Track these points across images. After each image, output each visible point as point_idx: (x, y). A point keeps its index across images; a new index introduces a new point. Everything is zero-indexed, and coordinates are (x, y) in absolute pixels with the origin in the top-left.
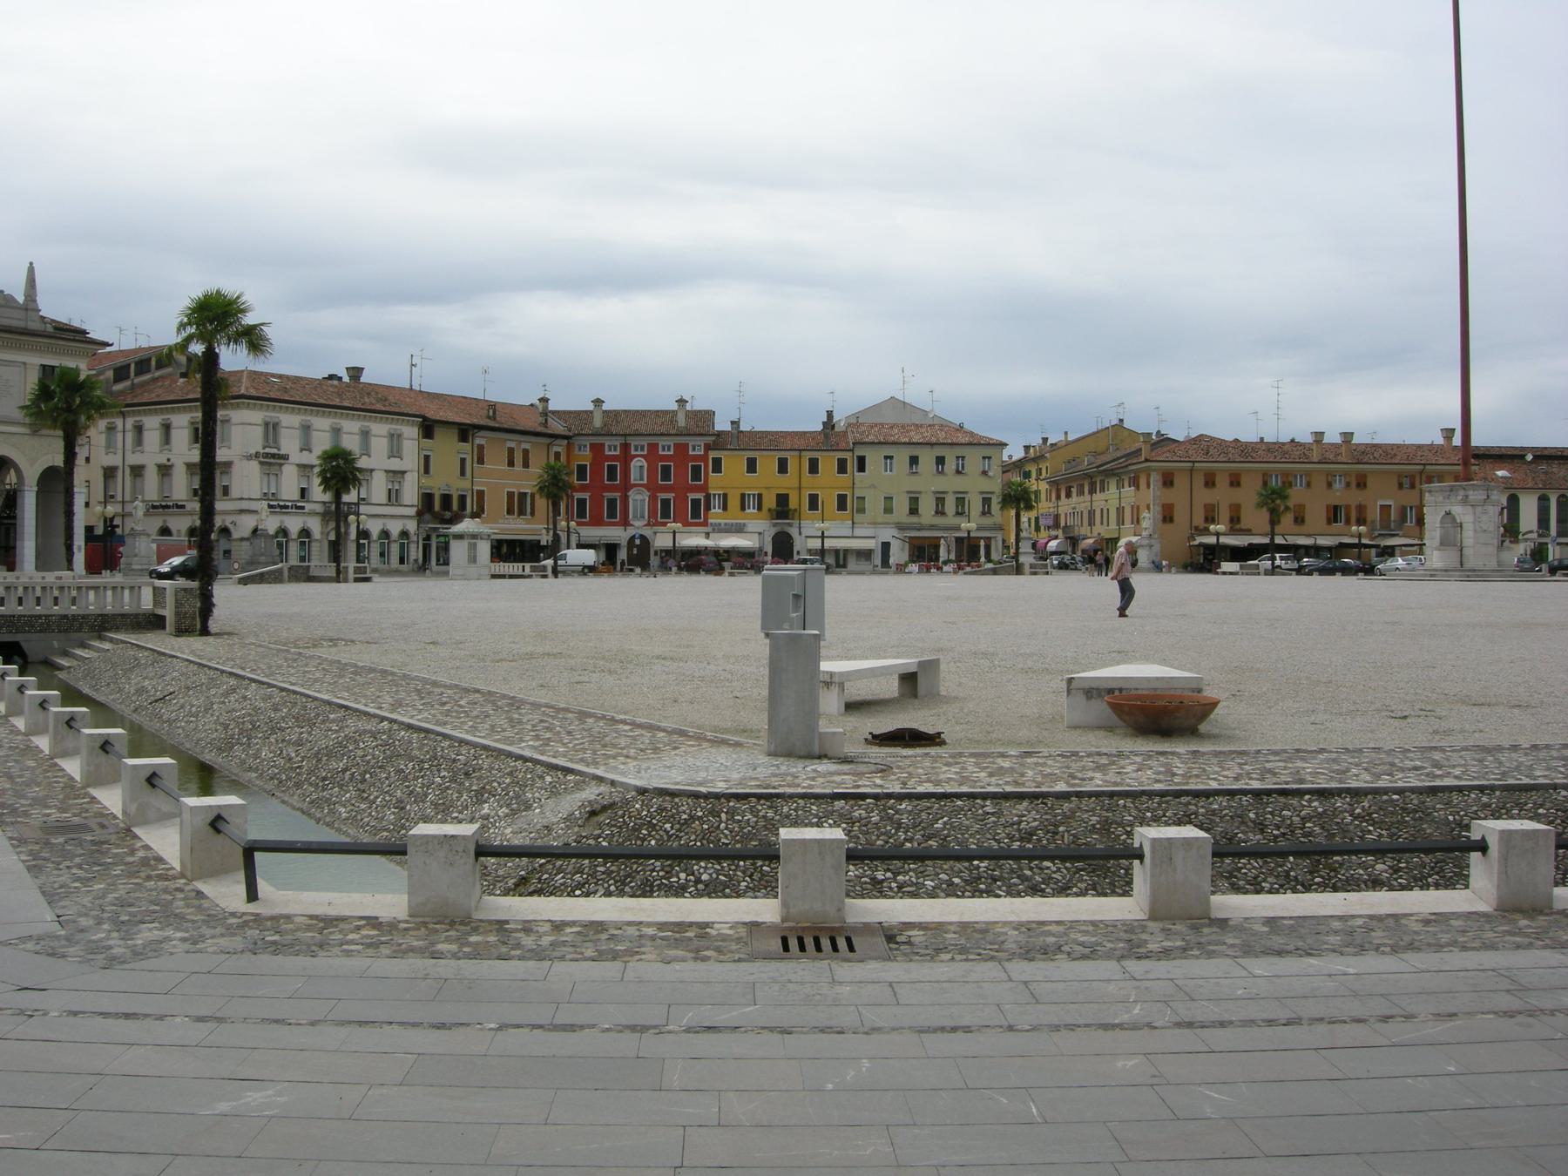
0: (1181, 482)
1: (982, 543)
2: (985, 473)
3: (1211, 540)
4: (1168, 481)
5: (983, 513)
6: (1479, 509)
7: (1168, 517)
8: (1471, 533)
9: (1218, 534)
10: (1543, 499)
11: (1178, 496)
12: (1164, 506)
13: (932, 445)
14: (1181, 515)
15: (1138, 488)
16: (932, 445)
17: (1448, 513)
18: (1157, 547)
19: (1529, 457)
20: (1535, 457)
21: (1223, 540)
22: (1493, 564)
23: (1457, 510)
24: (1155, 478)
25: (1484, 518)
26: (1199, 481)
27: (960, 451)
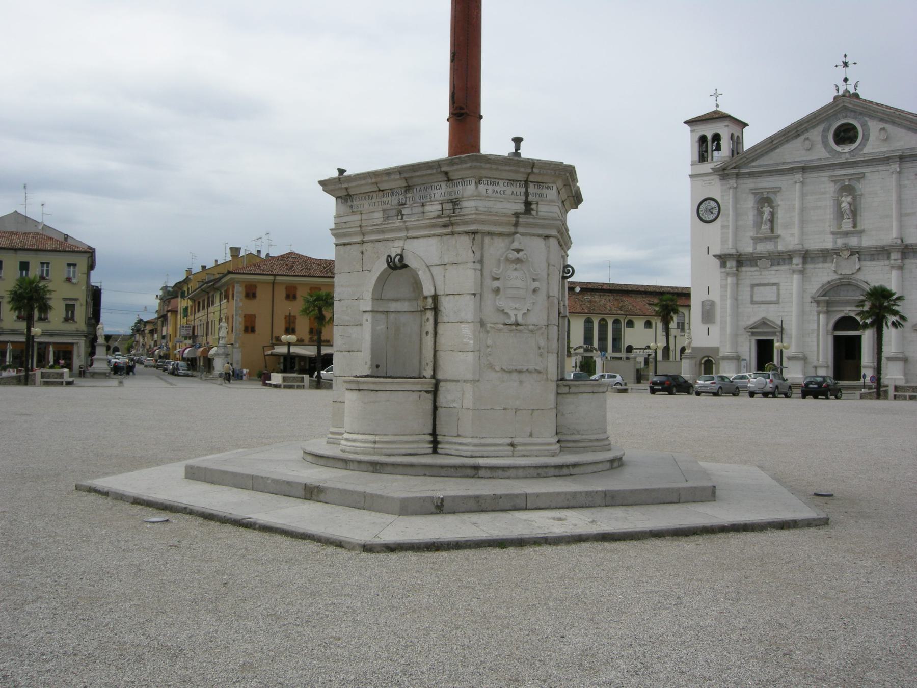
0: (263, 294)
1: (51, 349)
2: (69, 280)
3: (283, 350)
4: (250, 293)
5: (66, 320)
6: (496, 248)
7: (250, 328)
8: (467, 331)
9: (289, 344)
10: (589, 322)
11: (260, 307)
12: (245, 316)
13: (16, 250)
14: (262, 325)
15: (228, 299)
16: (16, 250)
17: (397, 265)
18: (237, 356)
19: (578, 289)
20: (581, 289)
21: (295, 350)
22: (541, 447)
23: (424, 252)
24: (239, 290)
25: (515, 278)
26: (281, 293)
27: (45, 258)
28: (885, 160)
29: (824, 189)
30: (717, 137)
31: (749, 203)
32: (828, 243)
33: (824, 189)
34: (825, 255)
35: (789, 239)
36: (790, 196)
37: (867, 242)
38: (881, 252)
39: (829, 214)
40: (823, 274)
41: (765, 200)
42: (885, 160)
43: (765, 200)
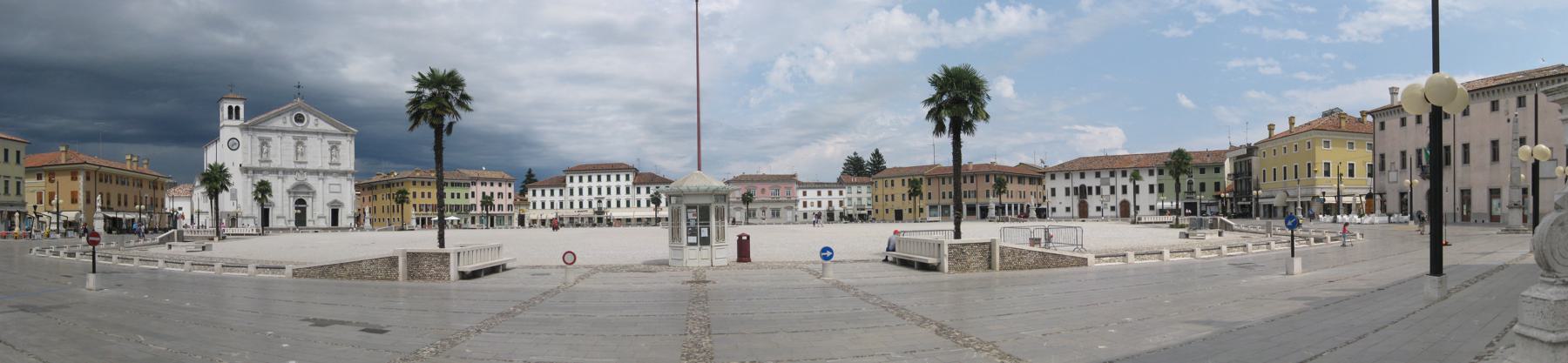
28: (317, 133)
29: (289, 140)
30: (237, 108)
31: (258, 143)
32: (292, 166)
33: (289, 140)
34: (293, 172)
35: (275, 164)
36: (275, 140)
37: (308, 167)
38: (317, 172)
39: (293, 153)
40: (291, 181)
41: (264, 142)
42: (317, 133)
43: (264, 142)
